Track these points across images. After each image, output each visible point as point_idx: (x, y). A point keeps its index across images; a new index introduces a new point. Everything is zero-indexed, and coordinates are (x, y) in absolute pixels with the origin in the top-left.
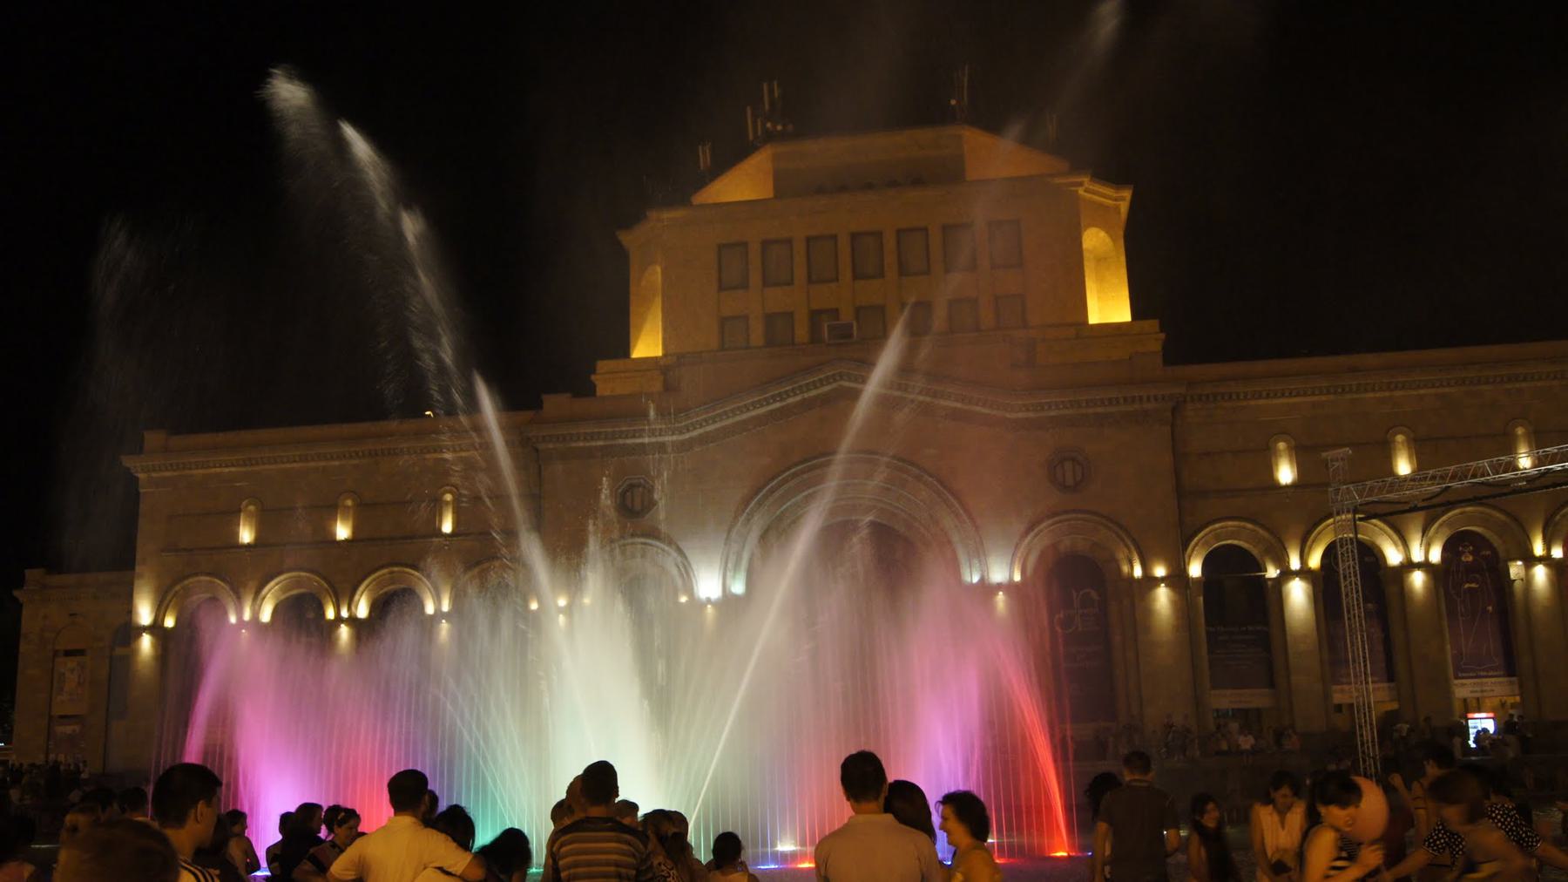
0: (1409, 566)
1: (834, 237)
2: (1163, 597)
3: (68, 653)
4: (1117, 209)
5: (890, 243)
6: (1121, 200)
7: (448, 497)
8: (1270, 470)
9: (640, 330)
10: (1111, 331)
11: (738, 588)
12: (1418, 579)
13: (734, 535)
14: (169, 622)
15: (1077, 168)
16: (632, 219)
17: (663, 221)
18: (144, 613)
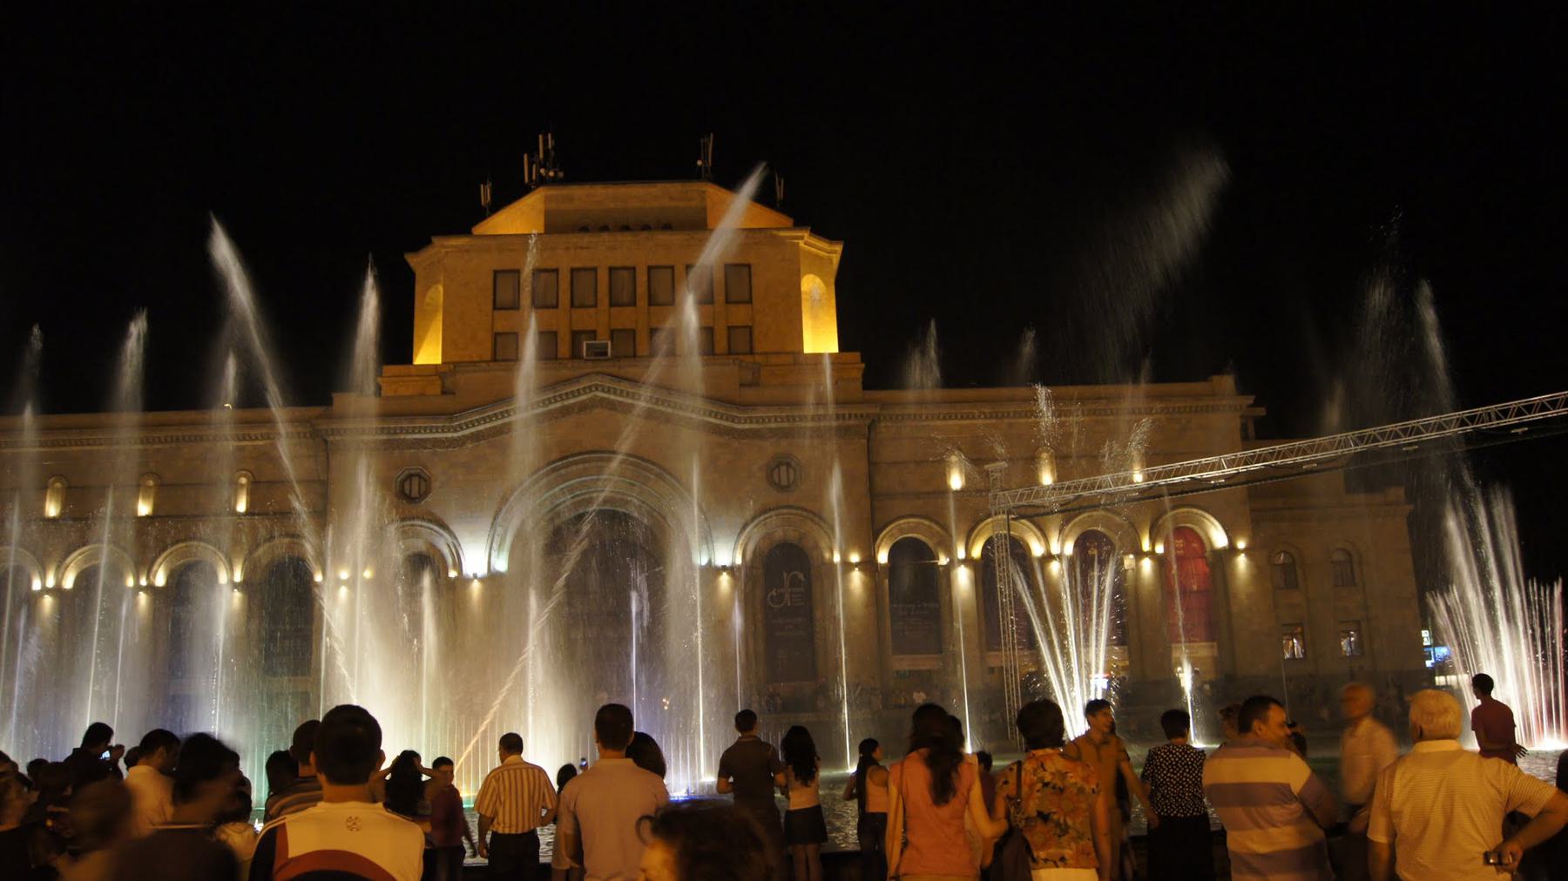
0: (1048, 557)
1: (594, 270)
2: (857, 577)
4: (830, 260)
5: (642, 278)
6: (833, 252)
7: (243, 481)
8: (943, 477)
9: (422, 340)
11: (501, 564)
13: (499, 520)
15: (799, 223)
16: (420, 243)
17: (445, 248)
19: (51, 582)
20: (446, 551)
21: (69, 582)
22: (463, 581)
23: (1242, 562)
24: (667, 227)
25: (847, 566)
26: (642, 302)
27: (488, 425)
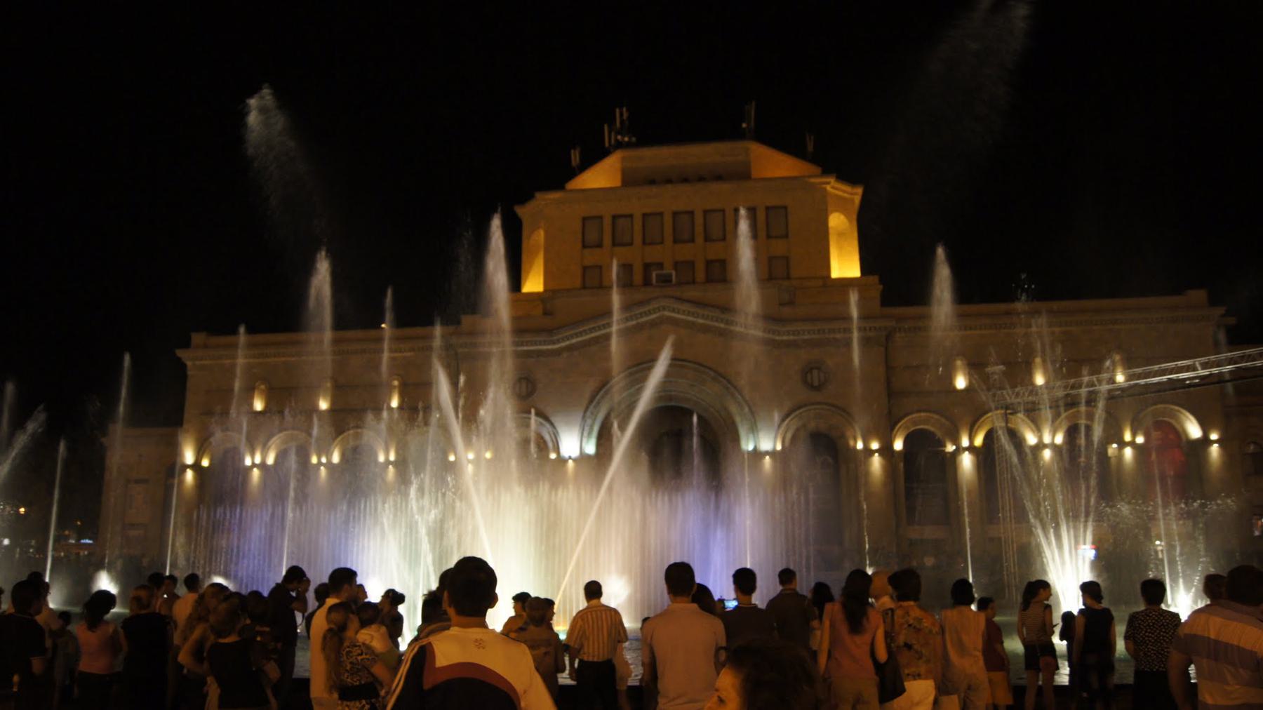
0: (1040, 446)
1: (661, 214)
2: (876, 462)
3: (137, 482)
4: (853, 201)
5: (699, 220)
6: (855, 194)
7: (396, 383)
9: (528, 273)
10: (846, 283)
11: (591, 449)
12: (1047, 454)
13: (588, 413)
14: (205, 463)
15: (826, 171)
16: (526, 198)
17: (545, 200)
18: (189, 457)
19: (258, 460)
20: (547, 437)
21: (270, 460)
22: (562, 461)
23: (1215, 449)
24: (719, 178)
25: (868, 452)
26: (700, 239)
27: (579, 339)
